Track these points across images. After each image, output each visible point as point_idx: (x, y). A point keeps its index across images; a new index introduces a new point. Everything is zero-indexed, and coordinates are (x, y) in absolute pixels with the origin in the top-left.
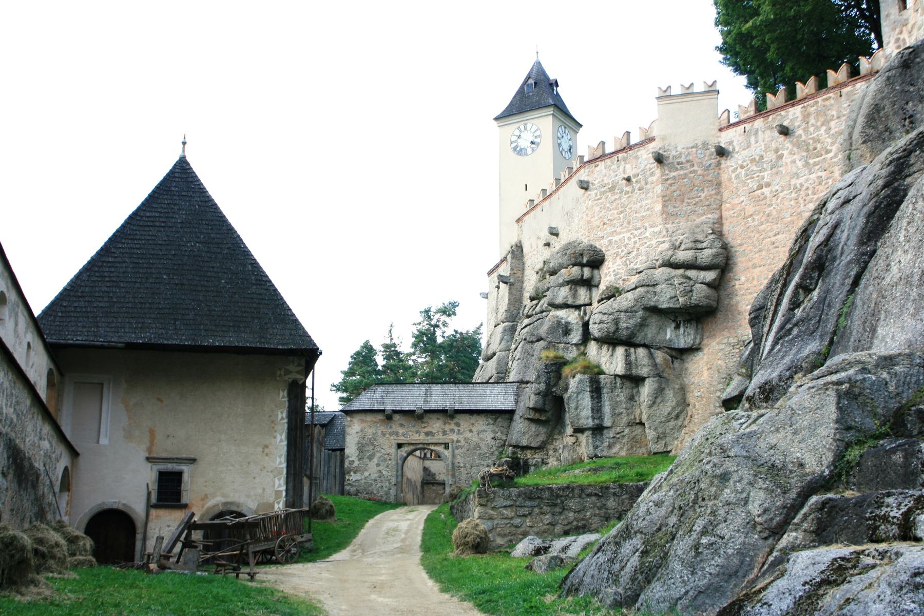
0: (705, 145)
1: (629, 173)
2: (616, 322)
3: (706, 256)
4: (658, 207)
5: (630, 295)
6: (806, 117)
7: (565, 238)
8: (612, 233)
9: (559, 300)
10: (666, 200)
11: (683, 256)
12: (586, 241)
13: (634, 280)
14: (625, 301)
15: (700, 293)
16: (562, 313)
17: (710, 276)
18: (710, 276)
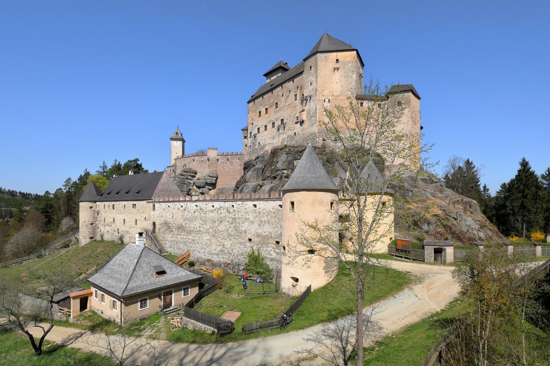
0: (215, 158)
1: (202, 160)
2: (201, 184)
3: (215, 175)
4: (208, 167)
5: (203, 180)
6: (231, 158)
7: (188, 166)
8: (199, 169)
9: (189, 178)
10: (209, 166)
11: (211, 175)
12: (194, 169)
13: (203, 177)
14: (201, 181)
15: (214, 181)
16: (189, 180)
17: (215, 179)
18: (215, 179)
